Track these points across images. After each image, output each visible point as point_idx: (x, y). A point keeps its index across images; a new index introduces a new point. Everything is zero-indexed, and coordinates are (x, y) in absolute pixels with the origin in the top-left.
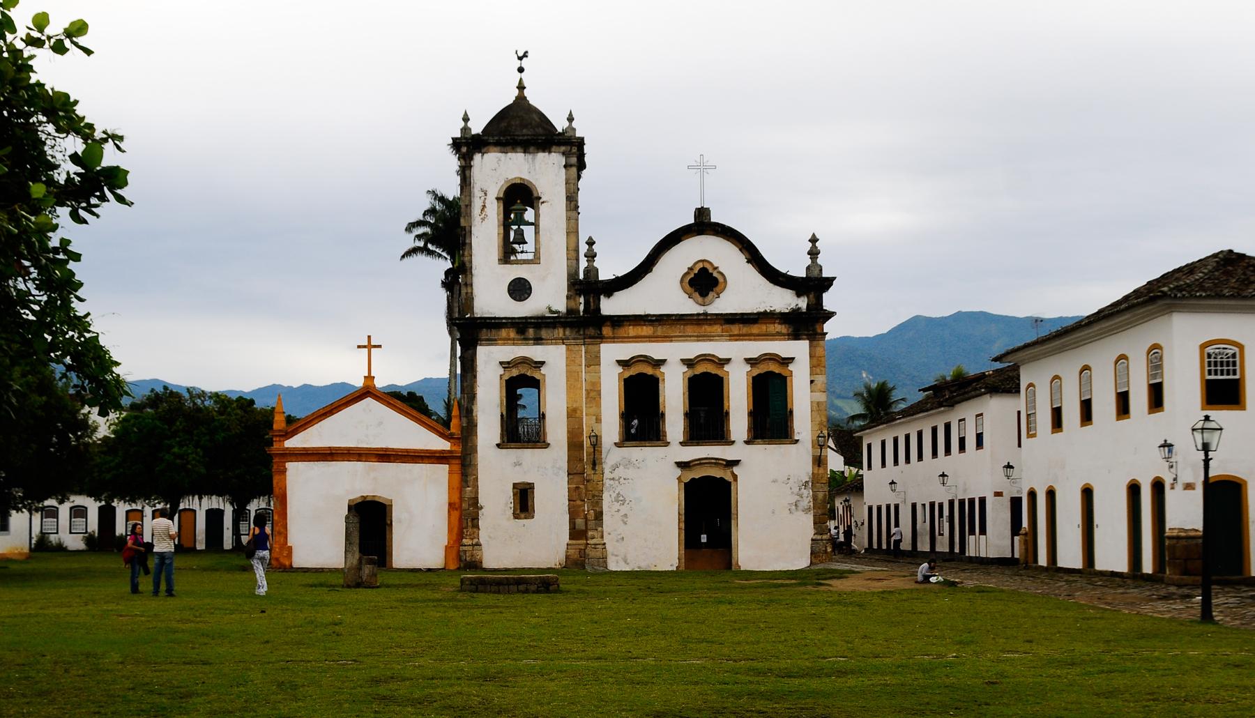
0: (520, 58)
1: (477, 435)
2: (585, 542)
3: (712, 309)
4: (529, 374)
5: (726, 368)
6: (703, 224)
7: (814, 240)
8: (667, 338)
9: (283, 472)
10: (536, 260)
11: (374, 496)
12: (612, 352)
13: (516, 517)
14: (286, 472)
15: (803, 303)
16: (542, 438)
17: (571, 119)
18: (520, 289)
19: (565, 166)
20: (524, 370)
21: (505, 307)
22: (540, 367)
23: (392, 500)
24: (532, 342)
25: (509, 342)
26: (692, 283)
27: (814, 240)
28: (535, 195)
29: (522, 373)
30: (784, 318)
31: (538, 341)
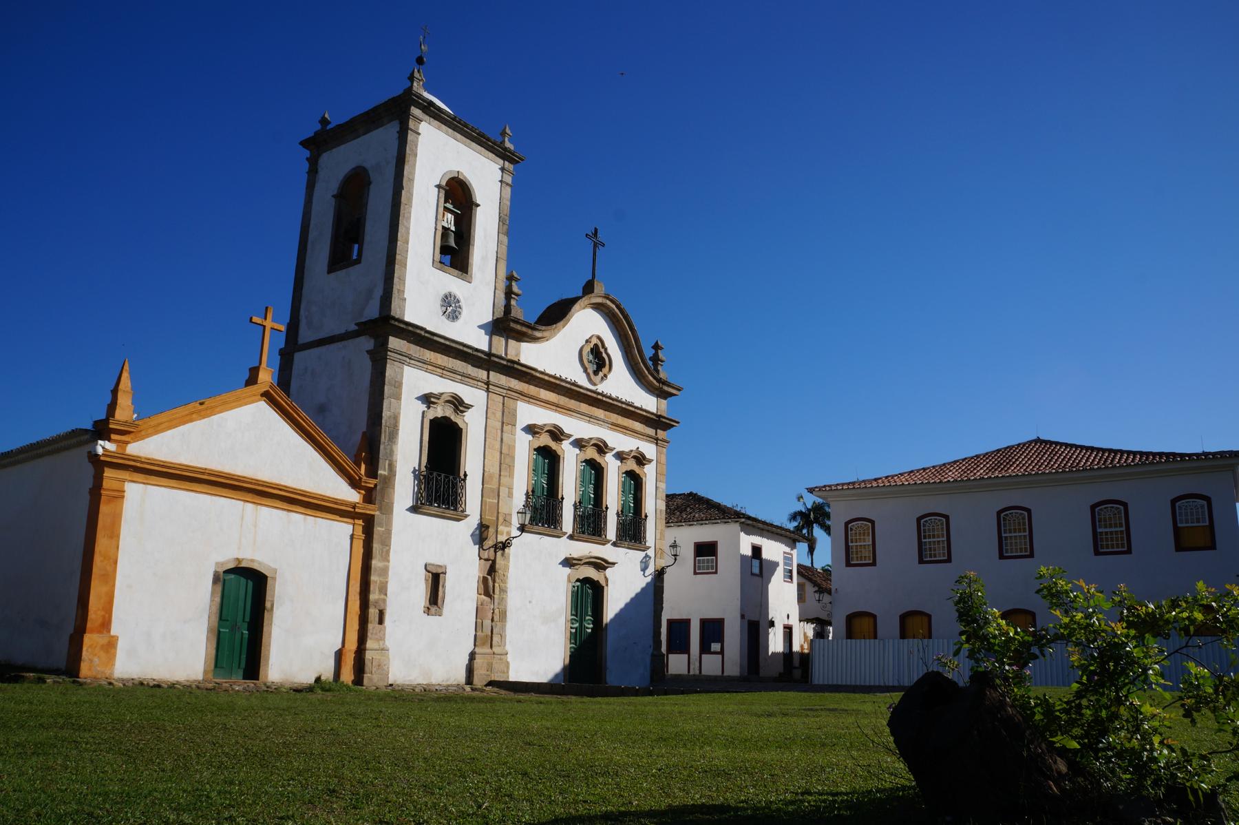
1: (394, 489)
2: (489, 650)
4: (453, 418)
9: (119, 495)
11: (252, 561)
12: (528, 413)
13: (428, 611)
14: (123, 497)
16: (463, 506)
18: (451, 306)
19: (501, 181)
20: (449, 412)
22: (465, 412)
23: (275, 571)
24: (460, 377)
25: (438, 370)
27: (656, 347)
28: (474, 200)
29: (447, 415)
31: (465, 378)
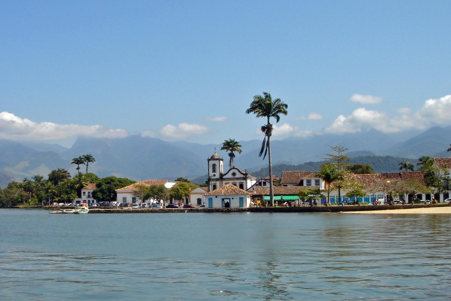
0: (215, 148)
3: (235, 177)
5: (237, 184)
6: (234, 168)
7: (246, 169)
8: (230, 180)
10: (216, 172)
15: (245, 176)
17: (220, 157)
18: (214, 175)
21: (213, 177)
26: (233, 174)
30: (243, 178)
